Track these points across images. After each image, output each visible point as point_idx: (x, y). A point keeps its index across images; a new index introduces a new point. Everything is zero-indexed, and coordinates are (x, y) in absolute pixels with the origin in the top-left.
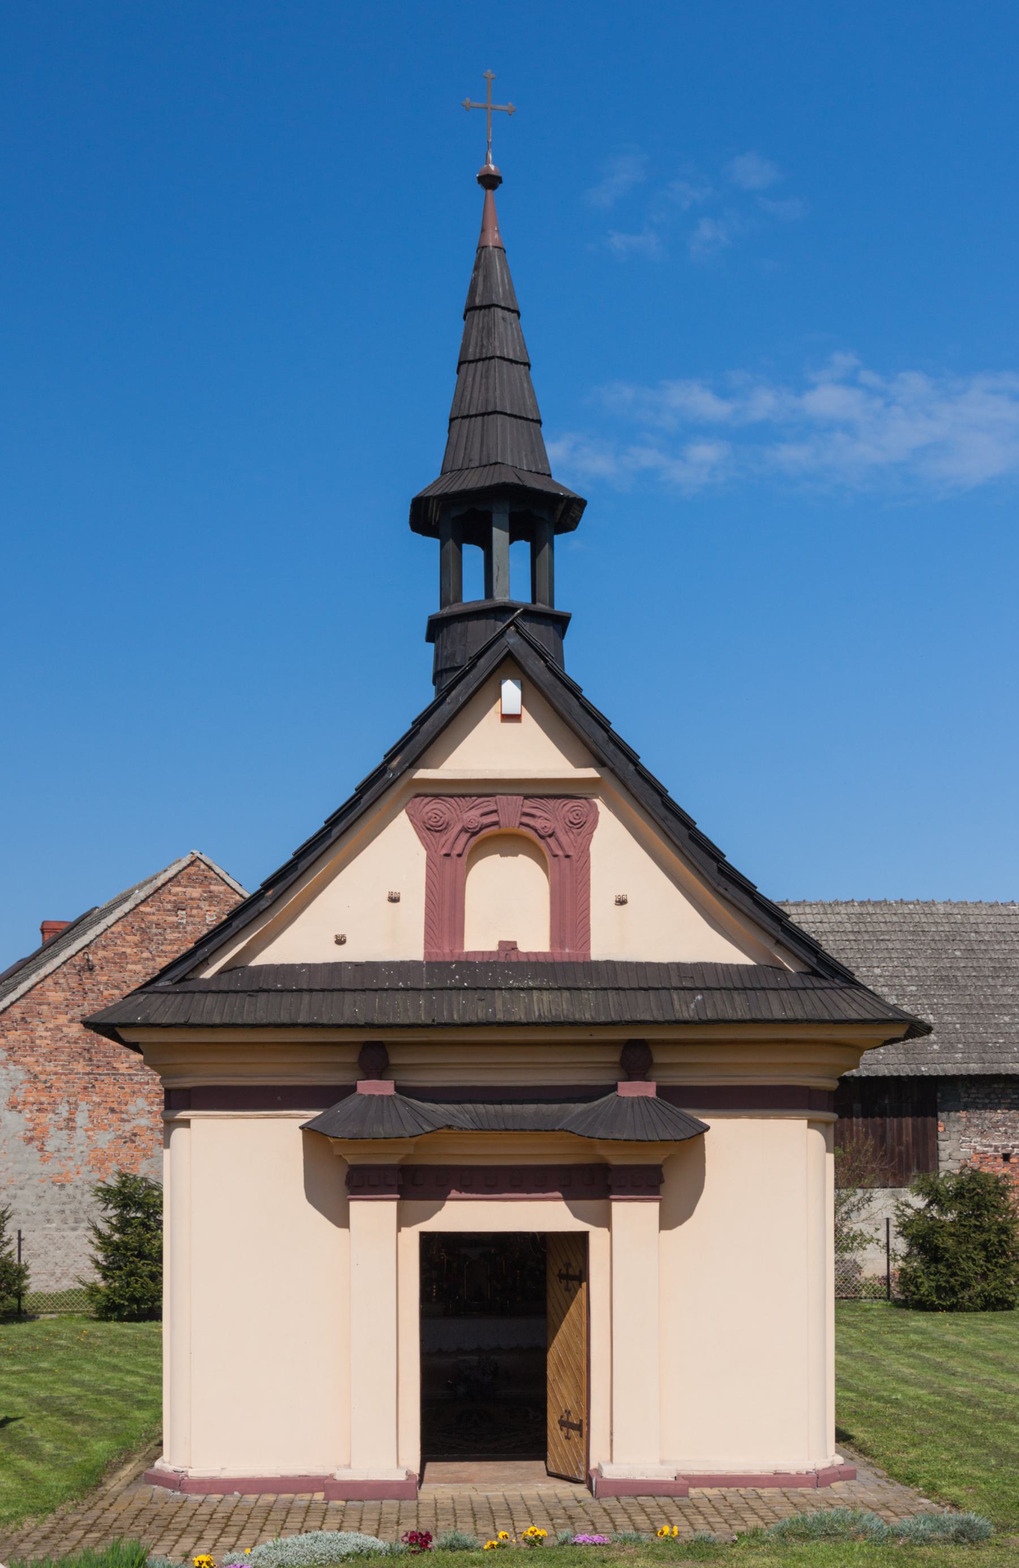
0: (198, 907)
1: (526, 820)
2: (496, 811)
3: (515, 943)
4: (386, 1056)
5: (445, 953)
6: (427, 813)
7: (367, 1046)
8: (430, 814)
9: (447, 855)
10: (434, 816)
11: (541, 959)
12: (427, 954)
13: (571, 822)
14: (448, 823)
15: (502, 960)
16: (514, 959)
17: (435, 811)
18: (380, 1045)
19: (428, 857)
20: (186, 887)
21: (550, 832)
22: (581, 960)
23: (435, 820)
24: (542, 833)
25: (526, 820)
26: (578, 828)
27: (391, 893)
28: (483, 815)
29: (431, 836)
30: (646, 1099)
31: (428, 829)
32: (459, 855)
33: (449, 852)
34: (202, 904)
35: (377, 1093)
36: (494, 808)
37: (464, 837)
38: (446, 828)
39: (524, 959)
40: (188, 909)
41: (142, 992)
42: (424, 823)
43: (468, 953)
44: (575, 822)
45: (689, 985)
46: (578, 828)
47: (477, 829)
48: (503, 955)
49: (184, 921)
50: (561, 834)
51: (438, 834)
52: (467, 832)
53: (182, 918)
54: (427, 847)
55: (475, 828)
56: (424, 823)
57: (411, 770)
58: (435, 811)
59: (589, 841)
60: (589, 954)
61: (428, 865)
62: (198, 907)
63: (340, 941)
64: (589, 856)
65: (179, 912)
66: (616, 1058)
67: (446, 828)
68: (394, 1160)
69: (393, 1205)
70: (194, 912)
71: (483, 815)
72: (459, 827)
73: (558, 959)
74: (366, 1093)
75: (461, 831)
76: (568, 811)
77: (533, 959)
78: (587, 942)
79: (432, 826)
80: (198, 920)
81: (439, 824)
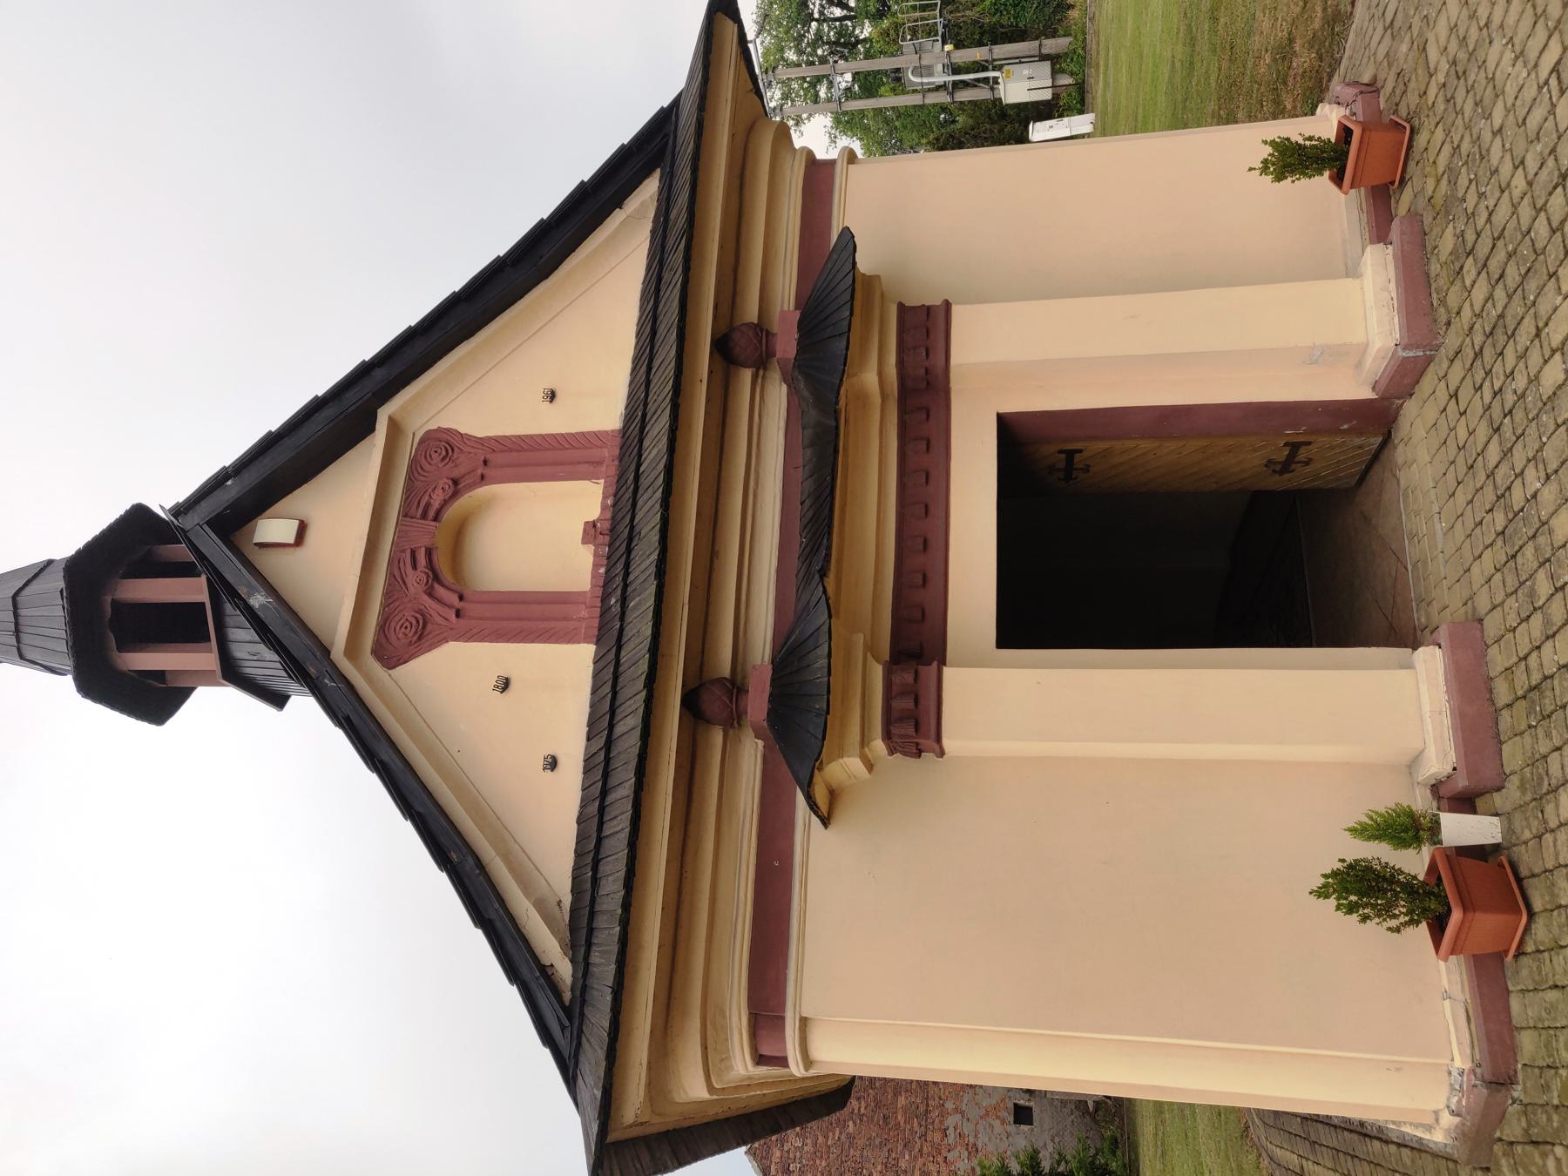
0: (788, 1152)
1: (432, 513)
2: (413, 553)
3: (587, 523)
5: (588, 616)
6: (398, 639)
8: (400, 636)
9: (458, 615)
10: (403, 629)
12: (586, 640)
13: (443, 459)
14: (417, 612)
16: (607, 525)
17: (398, 627)
19: (456, 640)
20: (771, 1162)
21: (450, 483)
22: (618, 441)
23: (409, 628)
24: (450, 492)
25: (432, 513)
26: (453, 450)
28: (415, 567)
29: (430, 636)
31: (420, 639)
32: (461, 598)
33: (454, 610)
34: (786, 1149)
36: (408, 553)
37: (440, 591)
38: (423, 615)
39: (609, 515)
40: (790, 1161)
42: (410, 644)
43: (593, 586)
44: (444, 453)
46: (453, 450)
47: (430, 573)
49: (798, 1166)
50: (456, 473)
51: (429, 627)
52: (432, 586)
53: (796, 1167)
54: (445, 640)
55: (428, 576)
56: (410, 644)
57: (332, 656)
58: (398, 627)
59: (469, 437)
60: (613, 431)
61: (468, 640)
62: (788, 1152)
63: (552, 763)
64: (490, 438)
65: (791, 1169)
67: (423, 615)
68: (878, 672)
69: (948, 673)
70: (791, 1156)
71: (415, 567)
72: (426, 598)
75: (430, 594)
76: (430, 464)
79: (416, 632)
80: (798, 1154)
81: (414, 622)
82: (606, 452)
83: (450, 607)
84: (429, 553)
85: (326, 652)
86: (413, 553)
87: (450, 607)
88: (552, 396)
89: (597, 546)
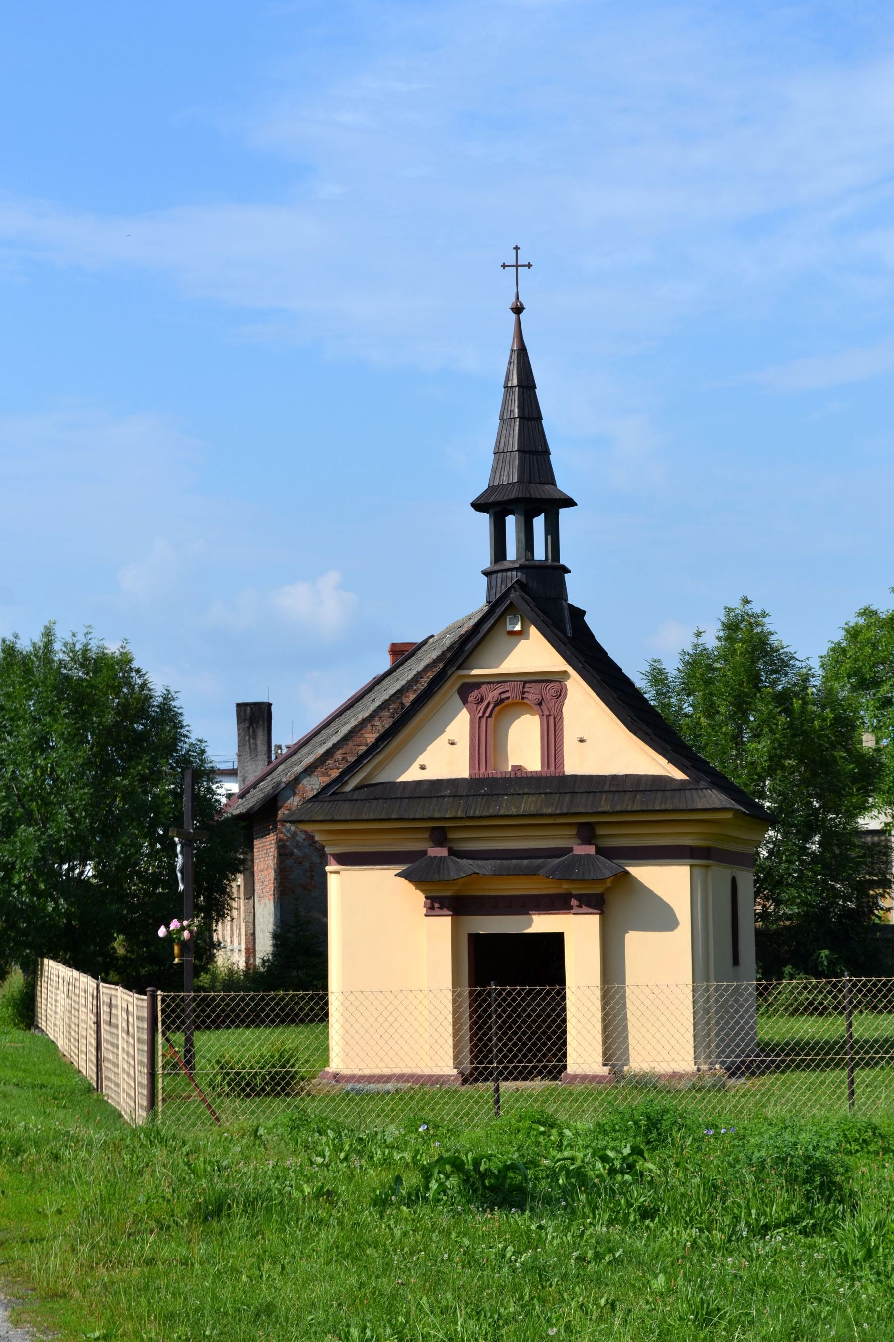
2: (507, 691)
4: (445, 833)
5: (482, 773)
7: (433, 828)
11: (535, 775)
12: (470, 774)
15: (513, 776)
16: (519, 775)
18: (442, 828)
22: (557, 775)
27: (449, 740)
28: (500, 694)
30: (588, 856)
35: (439, 855)
41: (312, 802)
45: (614, 789)
48: (513, 774)
66: (574, 832)
68: (450, 893)
69: (450, 918)
73: (544, 775)
74: (433, 855)
77: (530, 775)
78: (562, 764)
82: (552, 769)
83: (484, 713)
84: (508, 698)
85: (459, 668)
86: (507, 691)
87: (484, 713)
88: (582, 741)
89: (510, 772)
